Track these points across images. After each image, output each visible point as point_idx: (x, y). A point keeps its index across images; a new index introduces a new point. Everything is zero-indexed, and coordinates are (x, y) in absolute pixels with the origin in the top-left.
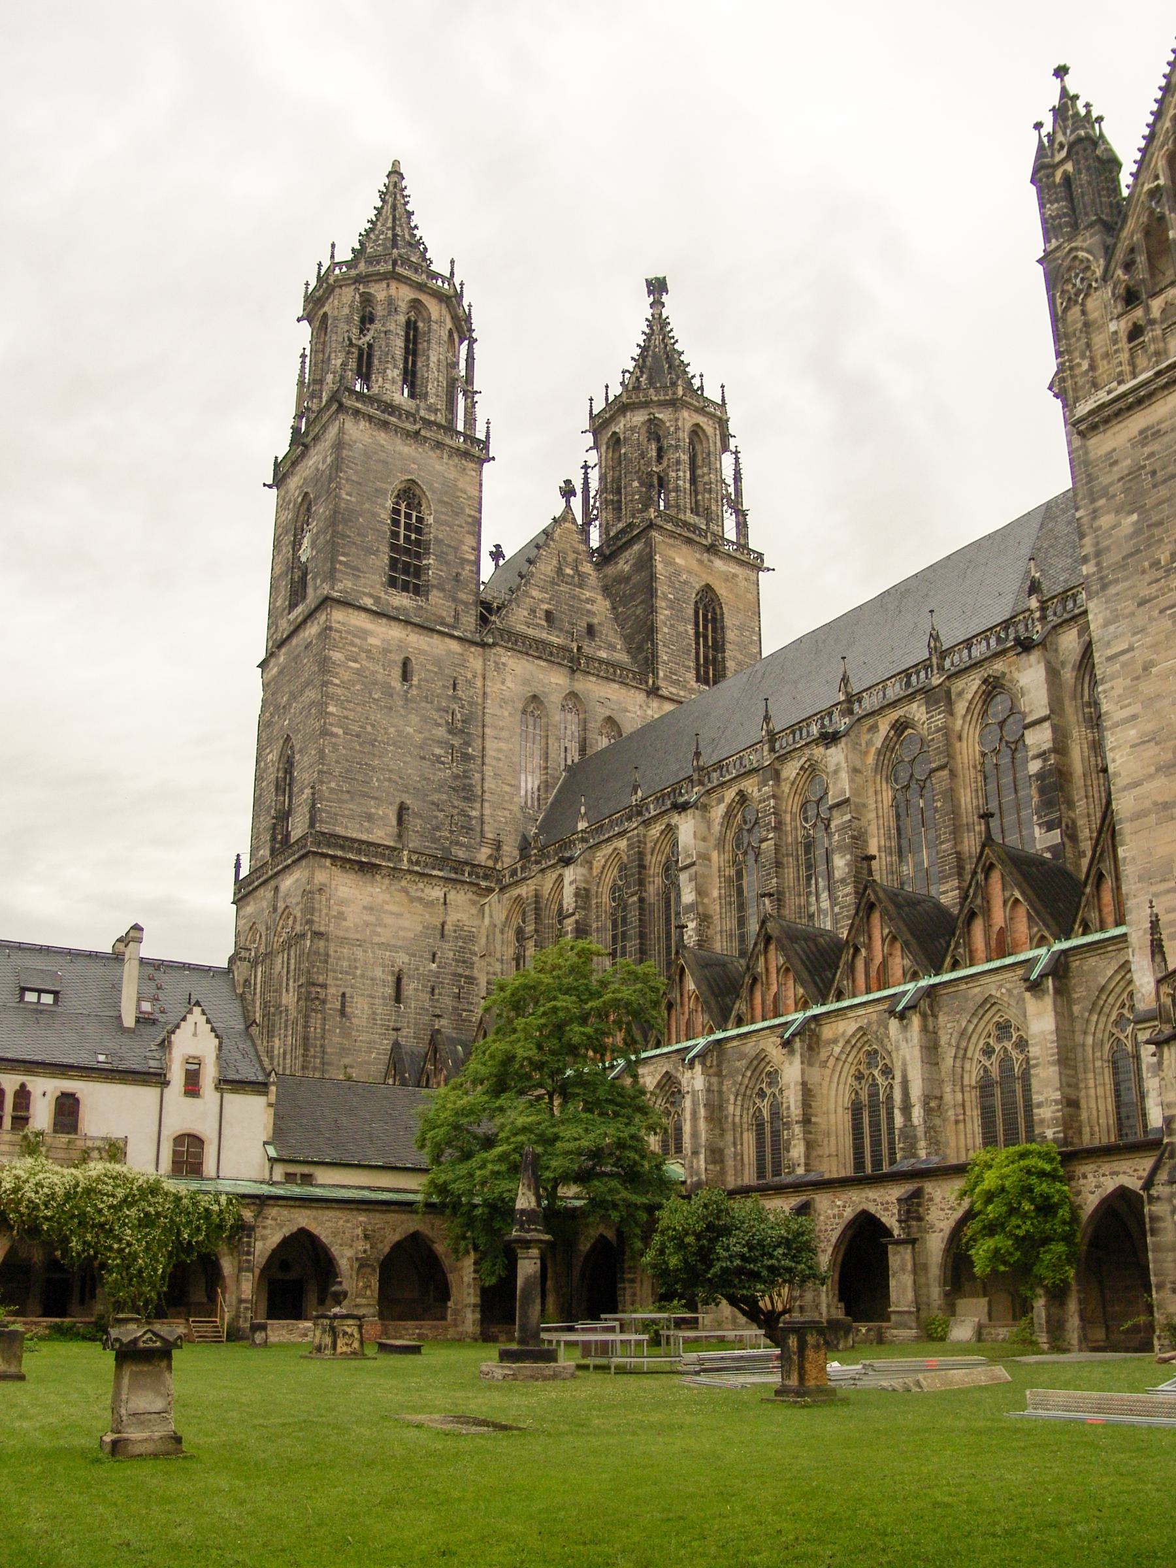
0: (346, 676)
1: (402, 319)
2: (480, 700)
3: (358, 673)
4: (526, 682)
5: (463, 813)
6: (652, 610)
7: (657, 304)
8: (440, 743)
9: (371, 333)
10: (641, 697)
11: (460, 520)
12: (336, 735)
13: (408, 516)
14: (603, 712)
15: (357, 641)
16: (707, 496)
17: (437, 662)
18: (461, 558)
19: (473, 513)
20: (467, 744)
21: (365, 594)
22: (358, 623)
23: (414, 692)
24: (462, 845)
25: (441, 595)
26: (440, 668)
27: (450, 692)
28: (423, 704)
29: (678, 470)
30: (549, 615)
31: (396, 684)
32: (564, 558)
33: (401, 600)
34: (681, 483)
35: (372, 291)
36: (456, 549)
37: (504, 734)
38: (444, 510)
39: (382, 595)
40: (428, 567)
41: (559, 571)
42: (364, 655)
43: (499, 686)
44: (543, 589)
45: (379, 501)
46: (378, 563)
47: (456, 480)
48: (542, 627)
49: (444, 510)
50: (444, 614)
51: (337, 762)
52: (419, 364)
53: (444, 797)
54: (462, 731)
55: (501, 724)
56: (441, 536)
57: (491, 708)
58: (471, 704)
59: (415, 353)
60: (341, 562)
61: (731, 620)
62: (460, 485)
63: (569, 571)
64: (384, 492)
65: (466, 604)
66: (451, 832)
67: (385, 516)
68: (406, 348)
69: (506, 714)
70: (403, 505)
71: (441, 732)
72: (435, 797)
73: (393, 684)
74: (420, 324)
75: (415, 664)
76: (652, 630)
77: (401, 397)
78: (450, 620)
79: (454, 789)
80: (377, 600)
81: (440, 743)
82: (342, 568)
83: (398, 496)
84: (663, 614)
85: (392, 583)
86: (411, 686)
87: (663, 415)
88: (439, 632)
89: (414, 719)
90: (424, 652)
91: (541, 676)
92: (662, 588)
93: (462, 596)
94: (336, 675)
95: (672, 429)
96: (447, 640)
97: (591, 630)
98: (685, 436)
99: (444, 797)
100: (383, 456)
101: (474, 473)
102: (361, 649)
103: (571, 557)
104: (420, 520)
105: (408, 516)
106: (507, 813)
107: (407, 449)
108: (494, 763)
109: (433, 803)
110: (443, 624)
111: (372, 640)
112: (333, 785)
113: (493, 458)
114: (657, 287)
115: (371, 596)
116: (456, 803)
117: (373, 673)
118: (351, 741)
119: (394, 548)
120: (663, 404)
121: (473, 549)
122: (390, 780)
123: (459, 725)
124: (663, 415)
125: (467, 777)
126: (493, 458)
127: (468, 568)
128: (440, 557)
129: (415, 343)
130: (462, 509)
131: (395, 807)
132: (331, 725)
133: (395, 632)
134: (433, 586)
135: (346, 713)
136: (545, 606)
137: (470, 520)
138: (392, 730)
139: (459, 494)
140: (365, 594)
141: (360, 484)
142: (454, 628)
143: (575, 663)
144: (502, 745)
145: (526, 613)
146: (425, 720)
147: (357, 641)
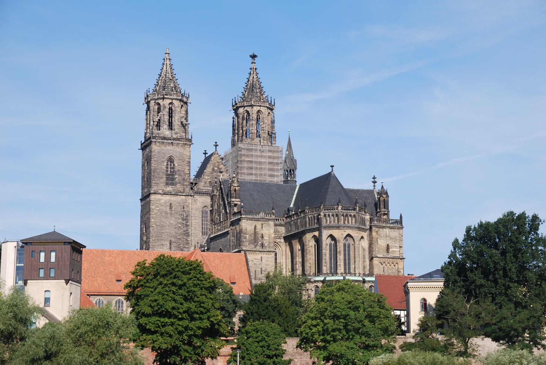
0: (155, 211)
1: (167, 110)
2: (191, 210)
3: (159, 210)
4: (203, 203)
5: (186, 240)
8: (180, 223)
9: (159, 116)
11: (185, 163)
12: (153, 227)
13: (171, 165)
15: (158, 202)
16: (262, 131)
17: (179, 203)
18: (185, 173)
19: (188, 160)
20: (187, 222)
21: (160, 189)
22: (158, 198)
23: (173, 212)
24: (186, 248)
25: (180, 185)
26: (180, 204)
27: (183, 210)
28: (176, 214)
29: (252, 127)
31: (168, 211)
32: (215, 165)
33: (169, 189)
34: (253, 131)
35: (159, 102)
36: (183, 171)
37: (197, 218)
38: (180, 161)
39: (164, 189)
40: (176, 178)
41: (213, 169)
42: (160, 205)
43: (195, 206)
44: (208, 176)
45: (162, 164)
46: (163, 181)
47: (183, 152)
48: (208, 186)
49: (180, 161)
50: (181, 189)
51: (154, 233)
52: (173, 120)
53: (181, 237)
54: (186, 219)
55: (196, 215)
56: (179, 169)
57: (194, 212)
58: (188, 211)
59: (172, 117)
60: (153, 183)
62: (184, 153)
63: (216, 169)
65: (186, 185)
66: (183, 245)
67: (164, 168)
68: (169, 116)
69: (197, 212)
70: (169, 163)
71: (180, 221)
72: (179, 237)
73: (167, 211)
74: (173, 108)
75: (173, 205)
78: (182, 191)
79: (184, 234)
80: (163, 190)
81: (180, 223)
82: (154, 184)
83: (168, 161)
85: (167, 184)
86: (172, 211)
87: (249, 109)
88: (179, 195)
89: (173, 218)
90: (176, 201)
91: (207, 200)
93: (185, 183)
94: (153, 212)
95: (251, 114)
96: (181, 196)
99: (181, 237)
100: (163, 151)
101: (188, 149)
102: (159, 204)
103: (217, 164)
104: (174, 165)
105: (171, 165)
106: (198, 238)
107: (169, 148)
108: (194, 226)
109: (179, 239)
110: (181, 192)
111: (162, 201)
112: (153, 239)
113: (193, 144)
115: (161, 189)
116: (184, 238)
117: (162, 209)
118: (157, 227)
119: (166, 175)
121: (188, 170)
122: (167, 235)
123: (185, 218)
124: (249, 109)
125: (187, 231)
126: (193, 144)
127: (187, 175)
128: (180, 175)
129: (172, 113)
130: (185, 160)
131: (169, 241)
132: (152, 224)
133: (167, 198)
134: (178, 183)
135: (156, 221)
136: (209, 180)
137: (187, 162)
138: (168, 223)
139: (184, 156)
140: (160, 189)
141: (157, 161)
142: (183, 193)
144: (196, 221)
145: (203, 184)
146: (176, 218)
147: (158, 202)
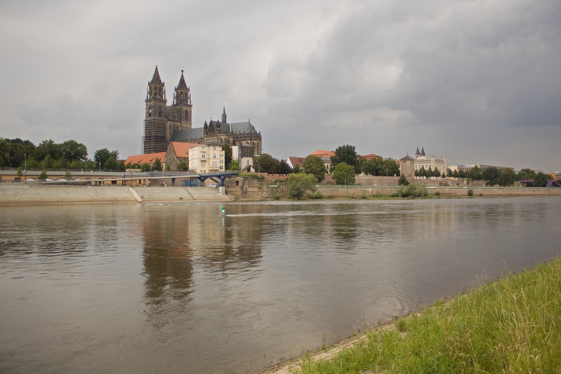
4: (170, 124)
6: (181, 114)
7: (182, 73)
10: (180, 123)
14: (176, 125)
30: (172, 117)
61: (189, 113)
64: (158, 108)
76: (181, 116)
77: (159, 97)
84: (182, 114)
92: (182, 111)
97: (176, 117)
98: (185, 93)
114: (182, 71)
119: (159, 113)
120: (183, 90)
128: (163, 113)
143: (174, 121)
